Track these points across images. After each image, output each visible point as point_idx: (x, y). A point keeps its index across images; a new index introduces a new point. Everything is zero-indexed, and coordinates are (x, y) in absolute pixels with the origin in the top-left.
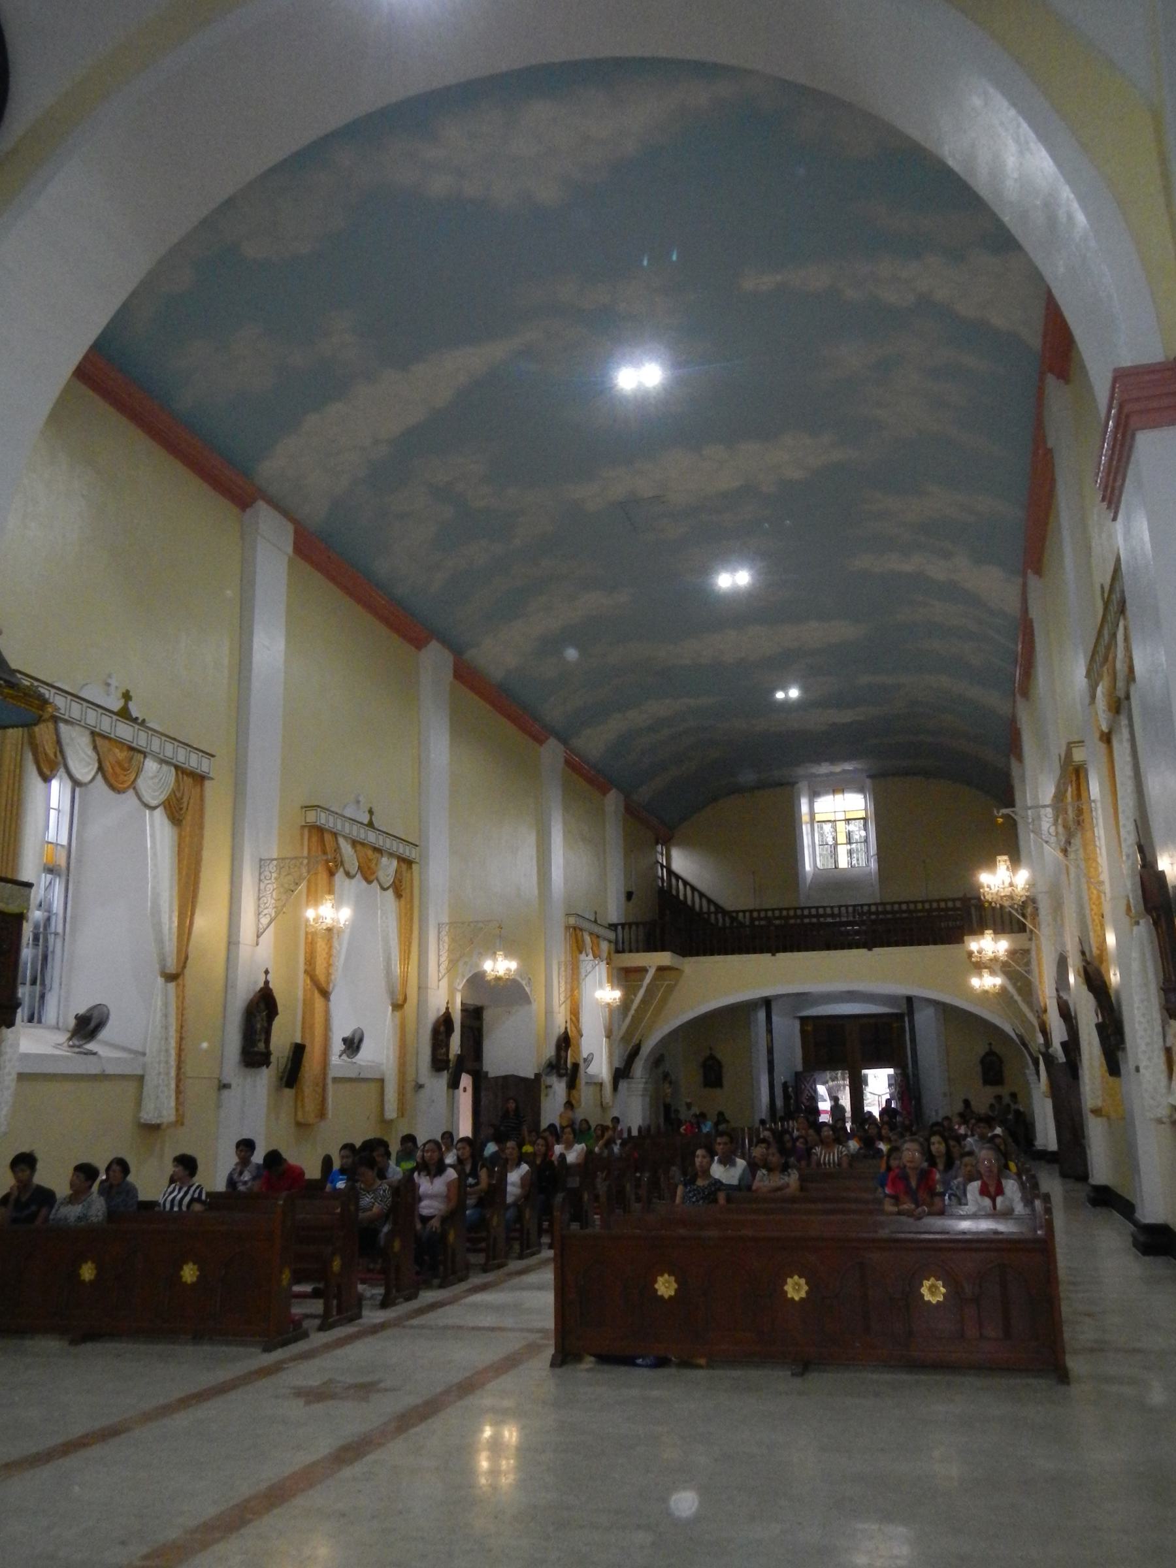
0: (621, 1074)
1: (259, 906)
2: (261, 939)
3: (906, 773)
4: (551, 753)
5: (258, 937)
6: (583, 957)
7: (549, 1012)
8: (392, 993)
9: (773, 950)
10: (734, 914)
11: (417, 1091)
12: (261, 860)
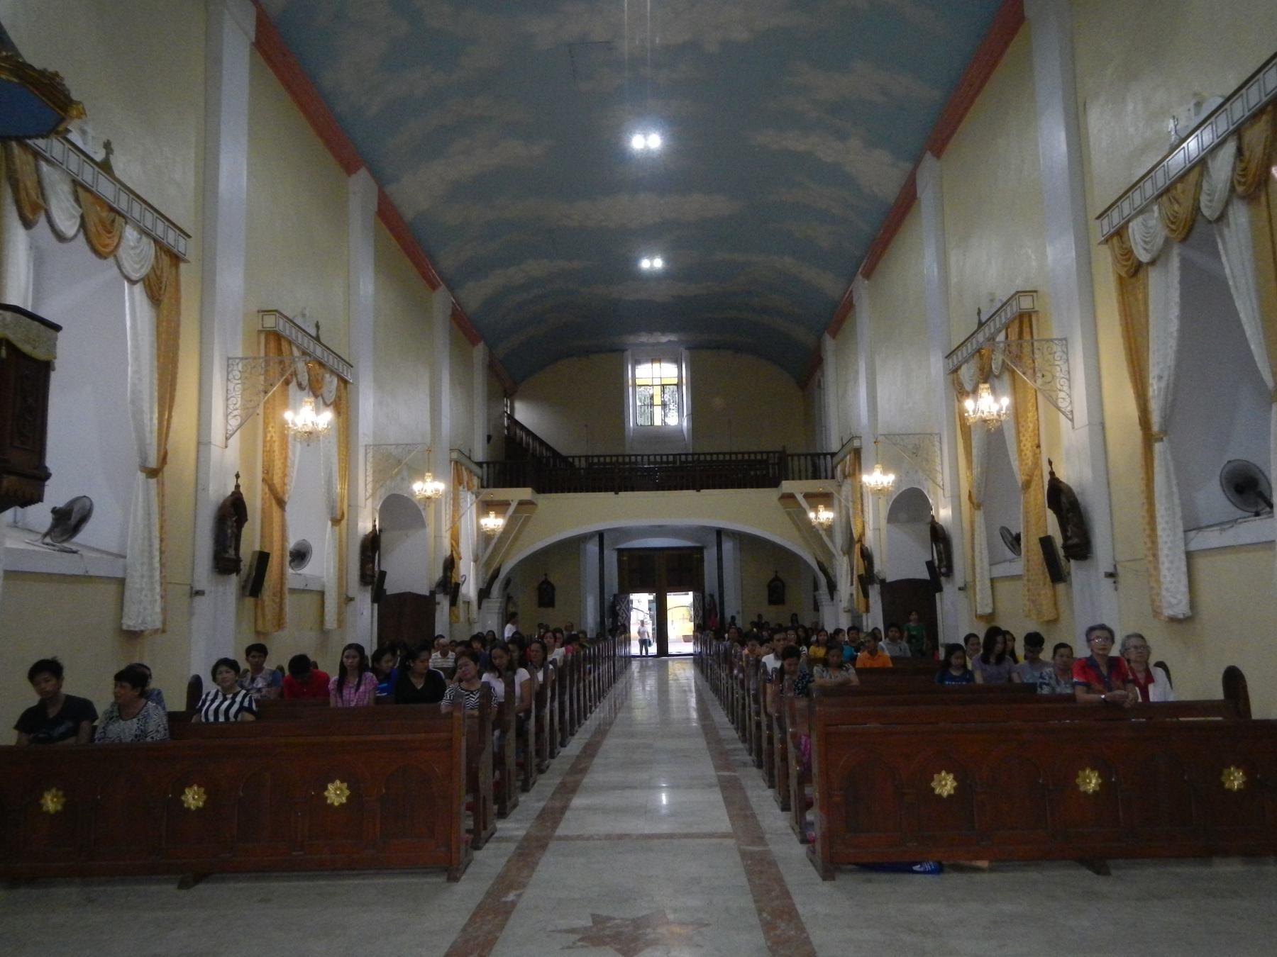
0: (484, 594)
1: (227, 407)
2: (230, 441)
3: (718, 347)
4: (441, 300)
5: (227, 439)
6: (461, 488)
7: (438, 537)
8: (332, 508)
9: (617, 489)
10: (571, 460)
11: (346, 604)
12: (229, 359)
